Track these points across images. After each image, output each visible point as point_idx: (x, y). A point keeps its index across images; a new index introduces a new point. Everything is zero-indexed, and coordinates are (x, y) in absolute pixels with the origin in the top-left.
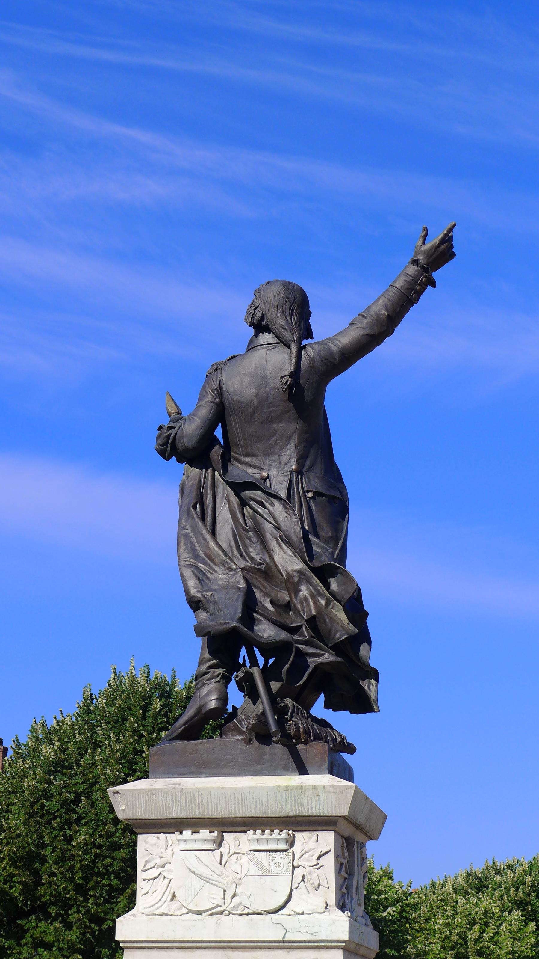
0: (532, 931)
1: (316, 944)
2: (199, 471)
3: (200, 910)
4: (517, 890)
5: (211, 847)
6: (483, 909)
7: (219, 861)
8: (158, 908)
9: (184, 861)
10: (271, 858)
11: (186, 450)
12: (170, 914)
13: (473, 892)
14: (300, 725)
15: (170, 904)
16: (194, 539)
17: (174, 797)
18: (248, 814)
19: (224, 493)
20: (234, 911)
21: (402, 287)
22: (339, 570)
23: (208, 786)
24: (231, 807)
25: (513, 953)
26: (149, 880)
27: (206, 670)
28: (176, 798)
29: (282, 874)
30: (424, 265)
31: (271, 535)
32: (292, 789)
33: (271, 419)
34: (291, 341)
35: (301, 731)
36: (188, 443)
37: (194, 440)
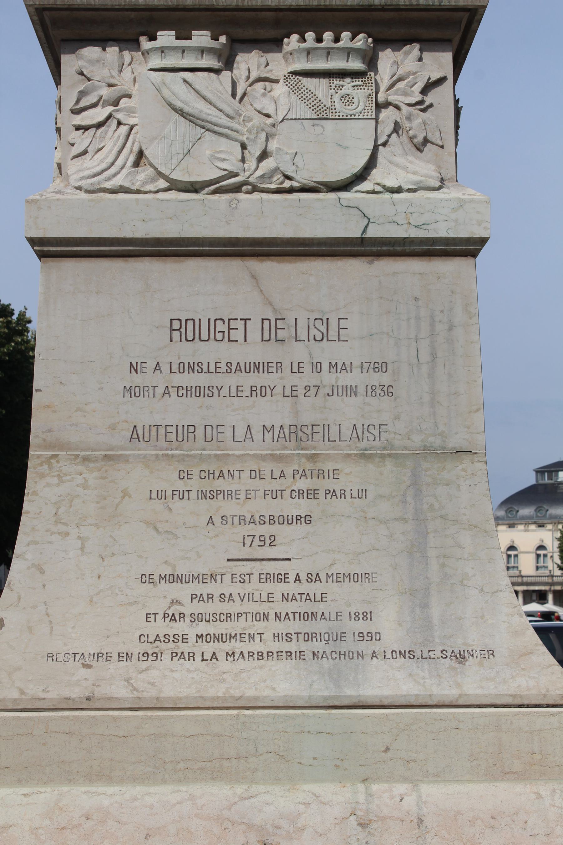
10: (333, 87)
12: (134, 188)
15: (134, 172)
29: (357, 117)
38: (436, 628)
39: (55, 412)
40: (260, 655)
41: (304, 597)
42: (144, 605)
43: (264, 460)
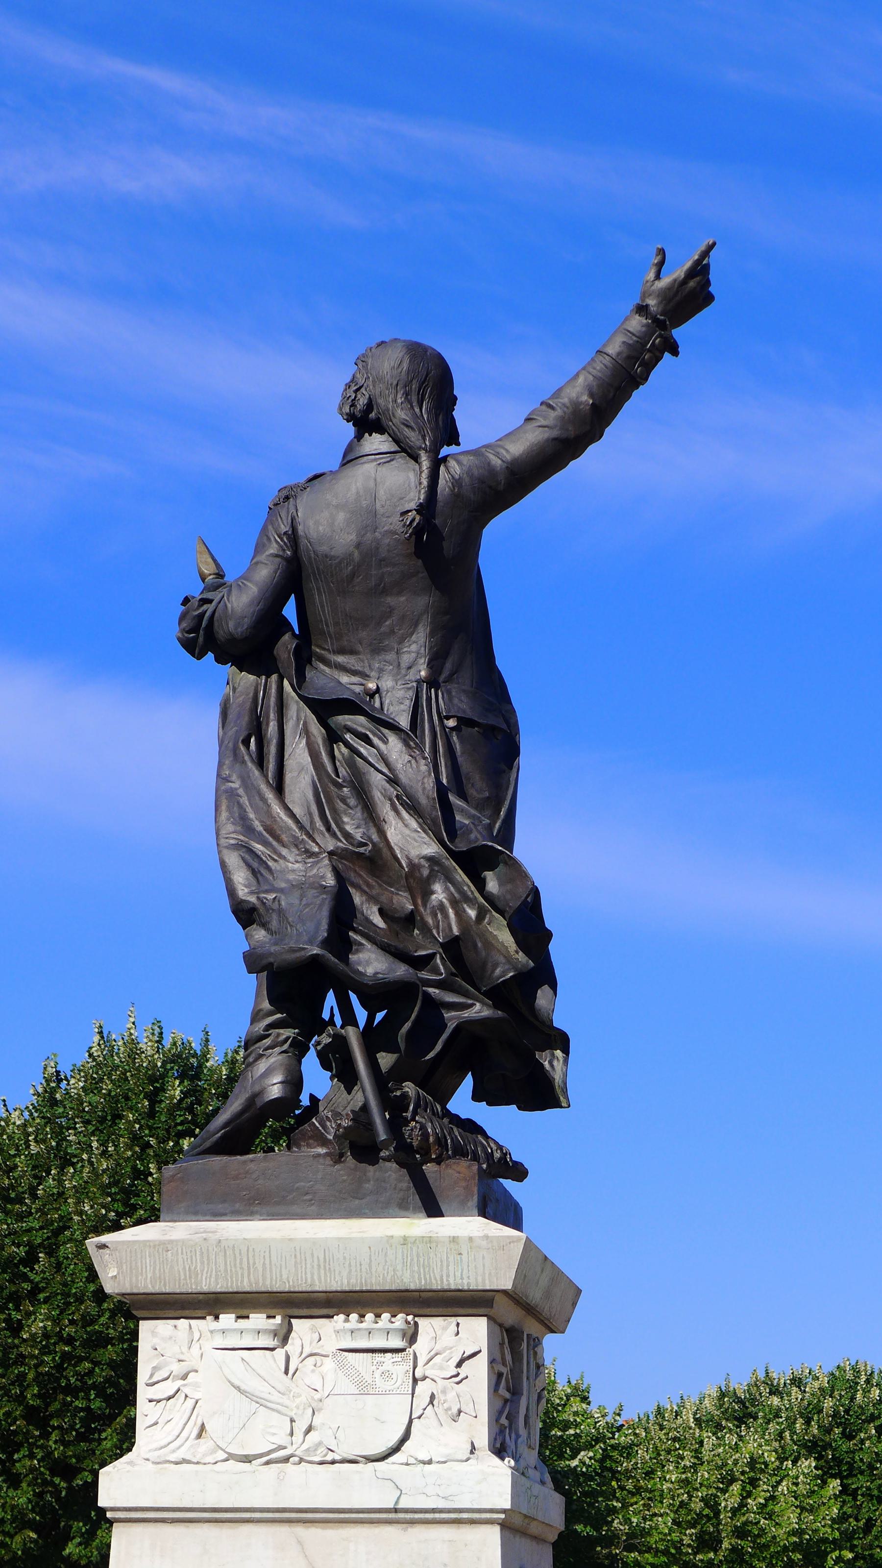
0: (835, 1494)
2: (254, 680)
3: (248, 1455)
4: (808, 1422)
5: (270, 1343)
6: (747, 1456)
7: (283, 1369)
9: (221, 1368)
10: (375, 1363)
11: (232, 640)
13: (729, 1425)
14: (430, 1130)
16: (245, 800)
17: (205, 1255)
18: (335, 1285)
19: (298, 719)
21: (619, 354)
22: (501, 857)
23: (265, 1235)
24: (306, 1273)
25: (799, 1533)
26: (159, 1401)
27: (264, 1031)
28: (208, 1256)
29: (394, 1392)
30: (658, 316)
31: (381, 793)
32: (415, 1242)
33: (384, 587)
34: (420, 448)
35: (431, 1139)
36: (236, 629)
37: (247, 622)
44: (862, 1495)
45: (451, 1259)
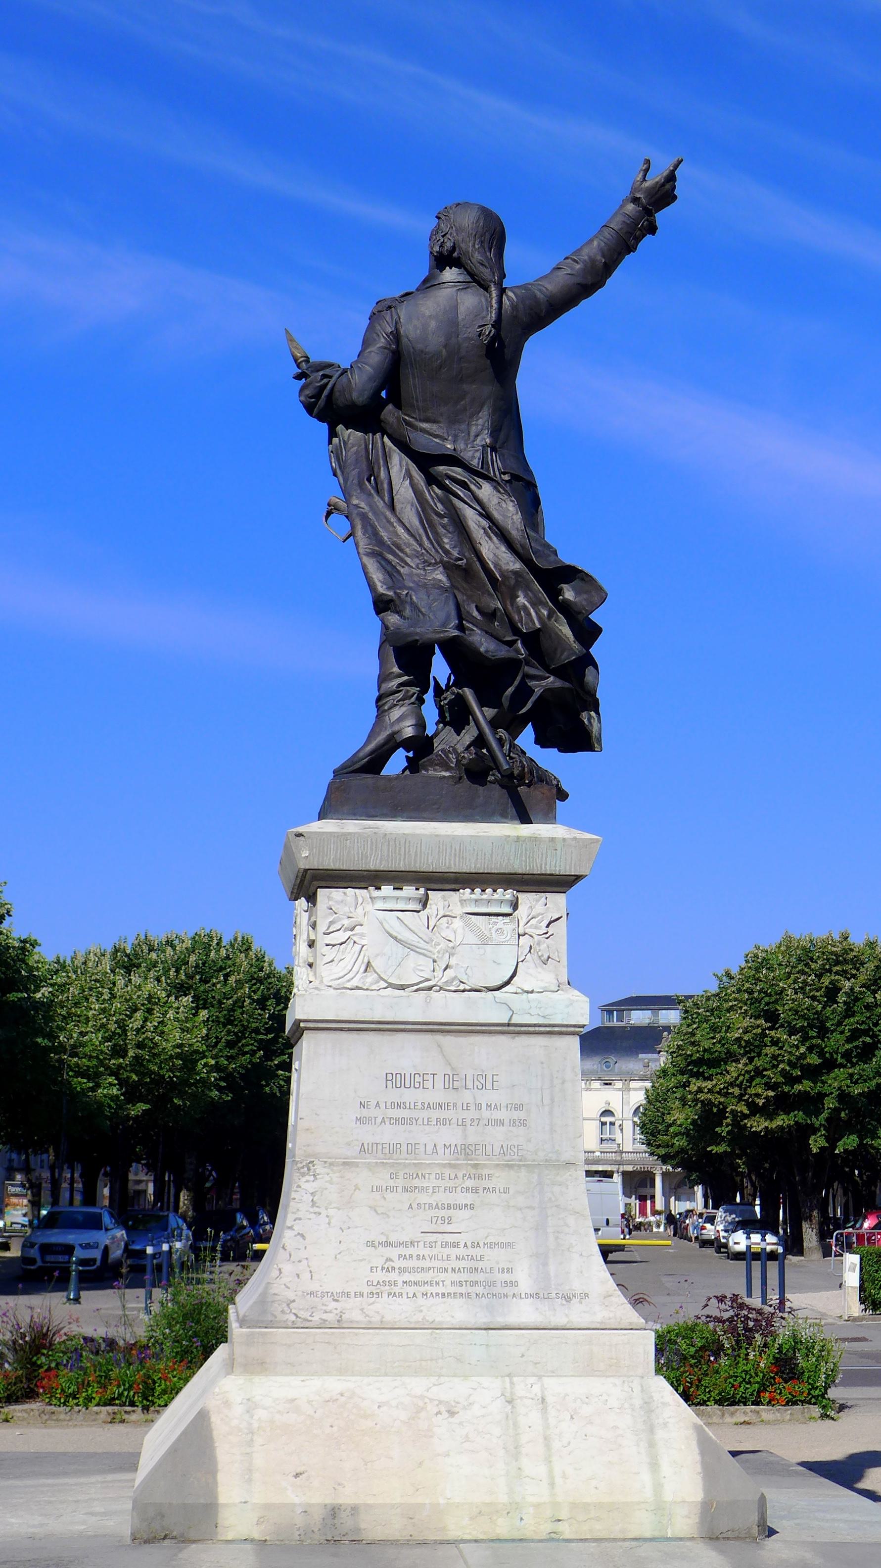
1: (548, 1029)
4: (177, 971)
8: (349, 981)
9: (381, 924)
11: (353, 406)
20: (447, 986)
21: (621, 229)
22: (579, 575)
23: (418, 832)
25: (180, 1046)
26: (334, 945)
34: (491, 281)
35: (526, 770)
38: (552, 1279)
39: (312, 1133)
40: (443, 1294)
41: (470, 1257)
42: (369, 1262)
43: (444, 1167)
44: (213, 1021)
45: (549, 854)
